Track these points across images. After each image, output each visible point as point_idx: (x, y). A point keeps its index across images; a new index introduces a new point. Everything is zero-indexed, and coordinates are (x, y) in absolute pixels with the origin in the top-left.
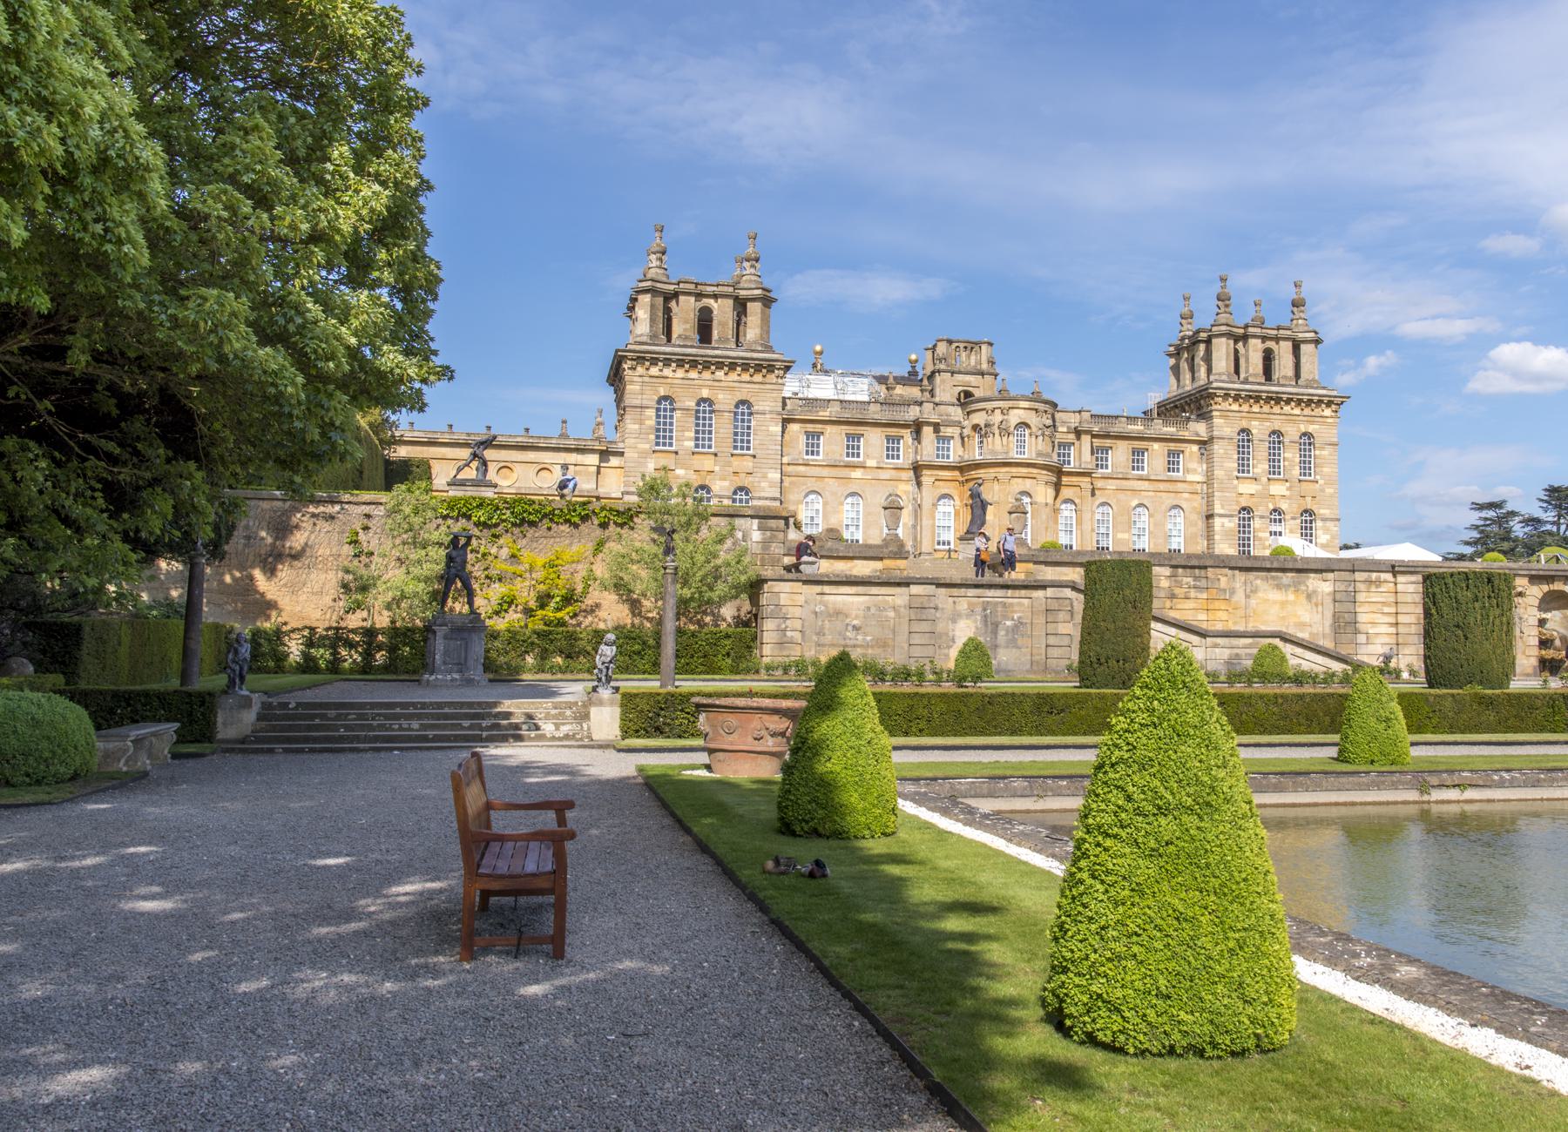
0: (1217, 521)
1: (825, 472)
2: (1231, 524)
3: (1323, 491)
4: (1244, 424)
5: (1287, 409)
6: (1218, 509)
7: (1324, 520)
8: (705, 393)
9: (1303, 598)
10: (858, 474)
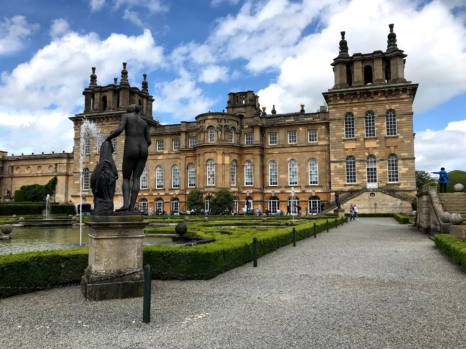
0: (332, 165)
3: (403, 142)
4: (348, 110)
5: (375, 98)
6: (332, 159)
10: (160, 157)
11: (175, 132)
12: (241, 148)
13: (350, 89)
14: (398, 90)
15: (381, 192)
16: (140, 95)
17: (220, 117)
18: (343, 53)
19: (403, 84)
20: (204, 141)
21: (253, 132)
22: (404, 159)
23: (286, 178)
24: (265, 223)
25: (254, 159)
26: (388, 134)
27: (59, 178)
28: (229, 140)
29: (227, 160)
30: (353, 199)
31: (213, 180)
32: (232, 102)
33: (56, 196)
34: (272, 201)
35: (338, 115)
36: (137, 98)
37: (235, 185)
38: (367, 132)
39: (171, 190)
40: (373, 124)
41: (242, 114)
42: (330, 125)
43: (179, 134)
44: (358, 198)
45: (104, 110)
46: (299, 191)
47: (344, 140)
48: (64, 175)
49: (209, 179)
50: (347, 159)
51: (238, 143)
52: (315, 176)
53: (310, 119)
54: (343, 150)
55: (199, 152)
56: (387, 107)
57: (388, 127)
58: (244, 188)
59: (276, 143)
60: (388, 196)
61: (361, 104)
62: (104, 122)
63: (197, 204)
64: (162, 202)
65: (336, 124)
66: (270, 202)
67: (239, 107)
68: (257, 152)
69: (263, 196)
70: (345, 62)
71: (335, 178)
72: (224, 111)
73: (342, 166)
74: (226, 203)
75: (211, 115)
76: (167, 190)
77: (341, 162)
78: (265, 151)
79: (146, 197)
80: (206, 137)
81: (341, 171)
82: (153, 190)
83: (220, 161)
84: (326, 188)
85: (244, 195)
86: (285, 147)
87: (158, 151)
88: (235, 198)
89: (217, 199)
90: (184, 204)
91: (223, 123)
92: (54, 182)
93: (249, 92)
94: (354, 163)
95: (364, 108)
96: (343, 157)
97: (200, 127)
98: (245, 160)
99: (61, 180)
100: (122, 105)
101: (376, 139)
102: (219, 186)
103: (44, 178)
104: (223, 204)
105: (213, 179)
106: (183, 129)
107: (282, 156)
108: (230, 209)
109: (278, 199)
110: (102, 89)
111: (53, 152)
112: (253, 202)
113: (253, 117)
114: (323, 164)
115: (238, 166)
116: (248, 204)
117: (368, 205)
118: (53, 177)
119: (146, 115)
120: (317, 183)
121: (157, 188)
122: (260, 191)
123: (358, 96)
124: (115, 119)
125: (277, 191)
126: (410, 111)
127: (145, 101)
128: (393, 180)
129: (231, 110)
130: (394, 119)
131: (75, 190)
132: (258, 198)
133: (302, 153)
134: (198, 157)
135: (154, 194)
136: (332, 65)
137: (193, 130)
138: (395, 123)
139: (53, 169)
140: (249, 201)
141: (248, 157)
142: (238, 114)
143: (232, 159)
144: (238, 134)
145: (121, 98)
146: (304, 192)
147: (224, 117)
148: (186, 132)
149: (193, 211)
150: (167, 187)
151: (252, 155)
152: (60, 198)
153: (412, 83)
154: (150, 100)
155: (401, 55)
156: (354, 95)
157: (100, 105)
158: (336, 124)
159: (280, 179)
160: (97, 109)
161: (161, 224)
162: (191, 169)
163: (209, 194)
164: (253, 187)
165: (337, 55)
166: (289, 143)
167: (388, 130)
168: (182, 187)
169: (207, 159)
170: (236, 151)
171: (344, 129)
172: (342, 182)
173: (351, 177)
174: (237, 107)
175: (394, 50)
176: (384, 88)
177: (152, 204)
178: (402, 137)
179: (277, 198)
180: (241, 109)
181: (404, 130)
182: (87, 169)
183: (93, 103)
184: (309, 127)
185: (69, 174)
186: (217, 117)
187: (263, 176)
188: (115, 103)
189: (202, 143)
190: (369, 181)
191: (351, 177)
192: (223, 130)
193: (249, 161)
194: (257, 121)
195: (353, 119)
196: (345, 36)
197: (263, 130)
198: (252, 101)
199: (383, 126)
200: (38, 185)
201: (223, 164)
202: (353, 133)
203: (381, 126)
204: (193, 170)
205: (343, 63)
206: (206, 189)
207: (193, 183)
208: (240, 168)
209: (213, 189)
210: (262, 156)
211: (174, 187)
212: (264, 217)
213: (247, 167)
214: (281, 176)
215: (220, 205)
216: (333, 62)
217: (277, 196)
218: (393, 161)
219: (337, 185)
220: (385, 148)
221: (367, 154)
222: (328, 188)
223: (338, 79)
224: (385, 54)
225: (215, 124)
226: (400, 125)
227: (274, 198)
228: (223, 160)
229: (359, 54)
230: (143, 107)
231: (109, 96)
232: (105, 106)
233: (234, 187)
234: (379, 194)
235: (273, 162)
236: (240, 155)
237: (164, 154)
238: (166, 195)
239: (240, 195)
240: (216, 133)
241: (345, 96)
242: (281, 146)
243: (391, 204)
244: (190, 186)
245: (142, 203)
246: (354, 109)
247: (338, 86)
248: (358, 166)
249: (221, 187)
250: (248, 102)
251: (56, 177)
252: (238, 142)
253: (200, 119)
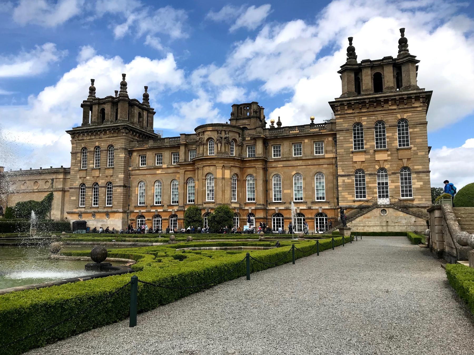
0: (340, 180)
1: (146, 172)
2: (351, 180)
3: (416, 154)
4: (357, 120)
5: (386, 106)
6: (340, 172)
8: (97, 144)
10: (159, 172)
11: (174, 144)
12: (243, 161)
13: (358, 98)
14: (411, 98)
15: (393, 208)
16: (140, 108)
17: (220, 128)
18: (351, 60)
19: (415, 91)
20: (203, 154)
21: (255, 145)
22: (418, 172)
23: (290, 193)
24: (262, 243)
25: (256, 173)
26: (400, 145)
27: (55, 194)
28: (229, 153)
29: (228, 174)
30: (362, 217)
31: (213, 195)
32: (236, 115)
33: (52, 213)
34: (276, 218)
35: (346, 126)
36: (136, 111)
37: (236, 201)
38: (377, 143)
39: (170, 206)
40: (384, 135)
41: (246, 126)
42: (338, 136)
43: (178, 147)
44: (368, 215)
45: (103, 122)
46: (304, 207)
47: (352, 152)
48: (60, 191)
49: (208, 194)
50: (356, 173)
51: (239, 156)
52: (322, 192)
53: (316, 130)
54: (351, 163)
55: (198, 166)
56: (399, 116)
57: (399, 138)
58: (246, 204)
59: (280, 156)
60: (401, 213)
61: (370, 113)
62: (102, 135)
63: (194, 221)
64: (160, 219)
65: (344, 135)
66: (274, 219)
67: (243, 119)
68: (259, 165)
69: (267, 213)
70: (352, 69)
71: (343, 194)
72: (227, 123)
73: (350, 181)
74: (226, 221)
75: (210, 126)
76: (166, 206)
78: (269, 165)
79: (143, 214)
80: (205, 150)
81: (348, 186)
82: (151, 206)
83: (219, 175)
84: (333, 204)
85: (246, 211)
86: (290, 160)
87: (156, 165)
88: (236, 214)
89: (216, 216)
90: (182, 221)
91: (223, 135)
92: (50, 198)
93: (253, 103)
94: (364, 177)
95: (374, 117)
96: (351, 170)
97: (199, 139)
98: (247, 174)
99: (57, 196)
100: (121, 117)
101: (387, 150)
102: (219, 202)
103: (40, 193)
104: (222, 221)
105: (213, 194)
106: (183, 142)
107: (286, 170)
108: (230, 227)
109: (283, 216)
110: (100, 101)
111: (51, 167)
112: (255, 219)
113: (255, 129)
114: (331, 178)
115: (239, 180)
116: (250, 221)
117: (379, 223)
118: (49, 193)
119: (146, 128)
120: (324, 199)
121: (155, 204)
122: (262, 207)
123: (367, 105)
124: (112, 131)
125: (282, 207)
126: (422, 121)
127: (145, 113)
128: (407, 196)
129: (234, 123)
130: (407, 130)
131: (71, 206)
132: (260, 214)
133: (308, 167)
134: (197, 171)
135: (152, 211)
136: (339, 72)
137: (193, 142)
138: (407, 133)
139: (49, 184)
140: (252, 218)
141: (250, 171)
142: (241, 127)
143: (232, 173)
144: (239, 146)
145: (119, 110)
146: (310, 208)
147: (224, 128)
148: (186, 145)
149: (189, 228)
150: (166, 203)
151: (254, 169)
152: (55, 214)
153: (426, 90)
154: (151, 113)
155: (413, 61)
156: (362, 103)
157: (98, 118)
158: (344, 135)
159: (284, 194)
160: (95, 122)
161: (145, 243)
162: (191, 184)
163: (208, 210)
164: (255, 203)
165: (344, 61)
166: (294, 156)
167: (400, 141)
168: (181, 204)
169: (206, 173)
170: (237, 164)
171: (352, 140)
172: (350, 198)
173: (361, 192)
174: (240, 119)
175: (405, 55)
176: (395, 96)
177: (149, 221)
178: (416, 148)
179: (281, 214)
180: (245, 121)
181: (417, 140)
182: (84, 184)
183: (92, 116)
184: (315, 138)
185: (66, 190)
186: (217, 128)
187: (266, 191)
188: (113, 115)
189: (201, 156)
190: (380, 197)
191: (361, 192)
192: (223, 142)
193: (251, 175)
194: (260, 133)
195: (362, 130)
196: (353, 42)
197: (266, 142)
198: (256, 112)
199: (395, 137)
200: (34, 201)
201: (223, 178)
202: (362, 144)
203: (393, 136)
204: (193, 185)
205: (351, 70)
206: (205, 206)
207: (192, 198)
208: (242, 183)
209: (212, 206)
210: (265, 170)
211: (173, 203)
212: (262, 236)
213: (249, 181)
214: (285, 191)
215: (219, 223)
216: (340, 69)
217: (281, 212)
218: (405, 175)
219: (345, 201)
220: (397, 160)
221: (377, 167)
222: (336, 204)
223: (346, 87)
224: (395, 59)
225: (215, 136)
226: (413, 135)
227: (279, 215)
228: (223, 174)
229: (368, 61)
230: (143, 120)
231: (108, 108)
232: (103, 118)
233: (235, 203)
234: (391, 210)
235: (277, 176)
236: (241, 169)
237: (162, 168)
238: (164, 211)
239: (241, 212)
240: (216, 145)
241: (353, 105)
242: (285, 159)
243: (404, 222)
244: (189, 202)
245: (140, 220)
246: (363, 118)
247: (346, 95)
248: (368, 180)
249: (221, 203)
250: (252, 114)
251: (52, 193)
252: (240, 155)
253: (199, 130)
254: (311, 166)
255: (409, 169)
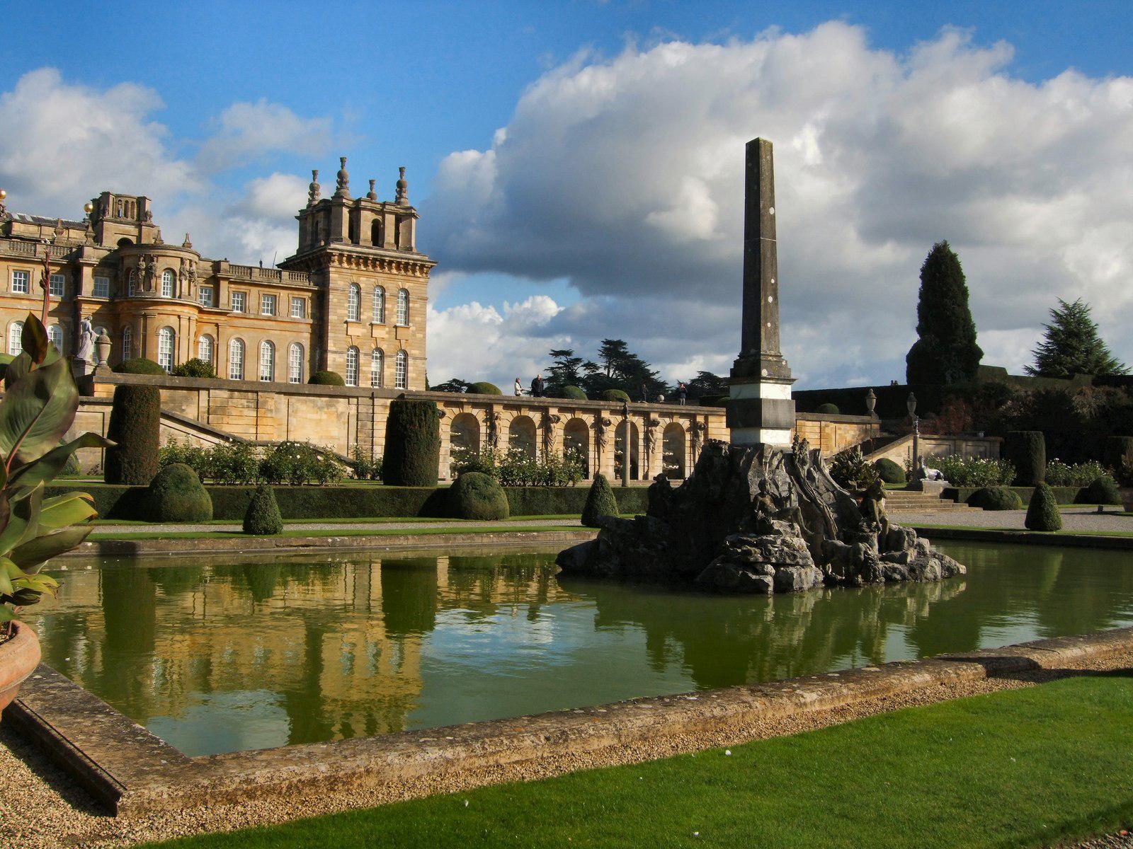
3: (414, 335)
4: (355, 279)
6: (331, 346)
7: (415, 358)
9: (334, 418)
22: (415, 358)
77: (341, 353)
176: (402, 258)
242: (252, 317)
254: (287, 333)
255: (406, 354)
